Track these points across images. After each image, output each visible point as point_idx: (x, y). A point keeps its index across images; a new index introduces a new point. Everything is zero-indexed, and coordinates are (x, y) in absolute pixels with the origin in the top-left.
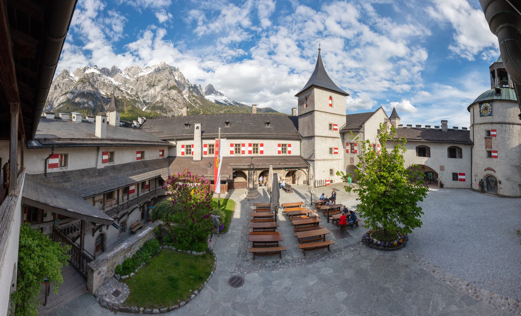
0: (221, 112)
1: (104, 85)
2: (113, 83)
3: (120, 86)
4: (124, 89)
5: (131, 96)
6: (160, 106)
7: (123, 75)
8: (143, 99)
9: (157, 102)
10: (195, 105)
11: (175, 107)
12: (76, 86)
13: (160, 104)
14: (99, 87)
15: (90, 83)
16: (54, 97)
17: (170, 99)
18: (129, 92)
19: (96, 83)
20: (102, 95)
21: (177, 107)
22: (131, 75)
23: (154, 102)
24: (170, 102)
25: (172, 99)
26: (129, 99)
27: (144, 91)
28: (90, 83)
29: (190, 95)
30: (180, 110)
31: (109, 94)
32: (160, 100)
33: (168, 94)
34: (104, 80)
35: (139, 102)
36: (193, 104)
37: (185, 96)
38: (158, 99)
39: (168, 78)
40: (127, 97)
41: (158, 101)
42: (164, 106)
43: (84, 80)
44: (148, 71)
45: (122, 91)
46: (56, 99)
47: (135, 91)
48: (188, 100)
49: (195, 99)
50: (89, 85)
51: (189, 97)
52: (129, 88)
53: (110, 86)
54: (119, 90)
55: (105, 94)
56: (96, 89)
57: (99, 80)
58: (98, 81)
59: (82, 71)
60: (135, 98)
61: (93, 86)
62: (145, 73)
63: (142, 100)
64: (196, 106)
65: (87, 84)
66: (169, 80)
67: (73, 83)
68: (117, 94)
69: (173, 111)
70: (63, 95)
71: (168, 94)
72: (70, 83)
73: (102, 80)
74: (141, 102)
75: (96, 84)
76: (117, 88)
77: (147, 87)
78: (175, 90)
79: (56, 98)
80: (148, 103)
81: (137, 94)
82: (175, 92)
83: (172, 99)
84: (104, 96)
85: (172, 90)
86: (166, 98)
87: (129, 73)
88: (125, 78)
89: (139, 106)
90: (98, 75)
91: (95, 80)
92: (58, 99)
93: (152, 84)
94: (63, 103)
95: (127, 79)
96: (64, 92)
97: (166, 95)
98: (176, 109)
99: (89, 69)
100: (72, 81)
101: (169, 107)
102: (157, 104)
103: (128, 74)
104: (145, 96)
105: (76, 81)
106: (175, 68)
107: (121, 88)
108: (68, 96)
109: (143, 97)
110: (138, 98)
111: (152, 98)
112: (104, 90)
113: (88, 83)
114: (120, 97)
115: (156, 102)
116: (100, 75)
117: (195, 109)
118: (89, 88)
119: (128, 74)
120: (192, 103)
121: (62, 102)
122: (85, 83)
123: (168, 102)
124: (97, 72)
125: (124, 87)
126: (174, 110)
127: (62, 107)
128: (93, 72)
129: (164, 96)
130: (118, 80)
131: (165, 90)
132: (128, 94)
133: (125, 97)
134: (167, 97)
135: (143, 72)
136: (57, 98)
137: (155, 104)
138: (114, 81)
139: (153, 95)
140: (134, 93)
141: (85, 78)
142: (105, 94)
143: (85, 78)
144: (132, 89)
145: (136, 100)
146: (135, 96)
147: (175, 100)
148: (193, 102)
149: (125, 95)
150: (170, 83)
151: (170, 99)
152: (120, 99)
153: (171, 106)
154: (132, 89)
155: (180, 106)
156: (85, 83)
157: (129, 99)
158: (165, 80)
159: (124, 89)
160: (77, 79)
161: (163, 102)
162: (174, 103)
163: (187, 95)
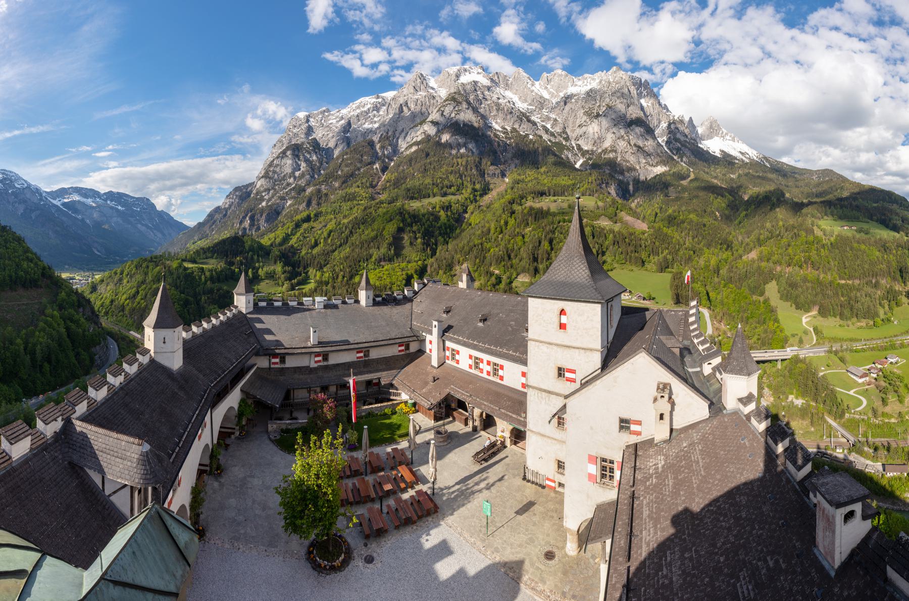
0: (732, 176)
1: (498, 110)
2: (517, 105)
3: (531, 112)
4: (539, 120)
5: (552, 134)
6: (610, 158)
7: (536, 91)
8: (578, 142)
9: (605, 151)
12: (442, 109)
13: (611, 155)
14: (488, 113)
15: (469, 103)
17: (630, 145)
18: (549, 126)
19: (481, 104)
20: (495, 130)
21: (644, 161)
22: (551, 90)
23: (600, 151)
24: (631, 151)
26: (550, 141)
27: (579, 126)
28: (469, 103)
29: (670, 138)
30: (650, 168)
31: (509, 129)
34: (499, 98)
35: (568, 149)
37: (660, 140)
38: (607, 144)
39: (625, 101)
40: (545, 137)
41: (606, 149)
42: (619, 159)
43: (457, 96)
44: (586, 85)
45: (534, 124)
46: (403, 135)
47: (562, 126)
48: (666, 149)
49: (680, 146)
50: (468, 109)
51: (668, 143)
52: (548, 118)
53: (511, 113)
54: (529, 121)
55: (500, 129)
56: (484, 117)
57: (488, 97)
58: (486, 100)
59: (454, 77)
60: (562, 139)
61: (475, 110)
62: (581, 88)
63: (574, 145)
64: (682, 161)
65: (465, 105)
66: (628, 106)
67: (435, 101)
68: (524, 129)
72: (430, 102)
73: (495, 98)
74: (573, 147)
75: (483, 106)
76: (524, 117)
77: (585, 118)
78: (640, 126)
79: (403, 131)
80: (587, 151)
81: (564, 132)
82: (640, 131)
84: (498, 133)
86: (623, 143)
87: (549, 86)
88: (541, 97)
89: (570, 156)
90: (485, 86)
91: (481, 96)
93: (595, 111)
94: (417, 143)
95: (545, 100)
98: (642, 165)
99: (467, 73)
100: (434, 98)
101: (628, 161)
102: (604, 155)
103: (546, 88)
105: (441, 98)
106: (641, 81)
107: (533, 118)
108: (426, 129)
109: (577, 139)
110: (567, 139)
111: (595, 142)
112: (499, 121)
113: (465, 103)
114: (531, 137)
115: (603, 151)
116: (489, 88)
117: (680, 168)
118: (467, 116)
119: (546, 88)
121: (414, 140)
122: (459, 103)
124: (484, 81)
125: (539, 116)
126: (638, 168)
127: (415, 152)
128: (476, 79)
129: (619, 138)
130: (525, 101)
132: (546, 130)
133: (541, 137)
134: (624, 140)
135: (576, 85)
137: (601, 153)
138: (519, 103)
139: (596, 135)
140: (558, 129)
141: (459, 93)
142: (500, 129)
143: (459, 93)
144: (555, 120)
145: (564, 143)
148: (677, 153)
149: (541, 132)
150: (631, 112)
151: (630, 145)
152: (531, 140)
154: (555, 120)
156: (459, 103)
157: (550, 141)
159: (539, 120)
160: (443, 93)
161: (616, 151)
163: (665, 138)
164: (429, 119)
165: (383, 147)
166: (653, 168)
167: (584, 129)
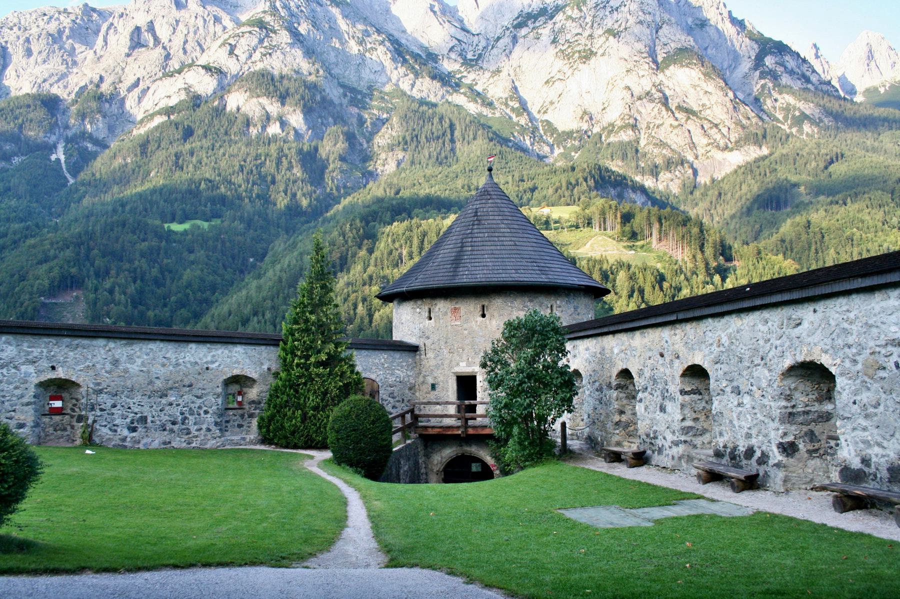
6: (621, 143)
9: (611, 129)
10: (794, 130)
11: (693, 146)
12: (233, 42)
13: (626, 136)
16: (130, 80)
21: (705, 141)
25: (679, 108)
36: (785, 127)
39: (649, 18)
42: (643, 143)
43: (268, 18)
46: (137, 92)
64: (801, 131)
65: (284, 37)
66: (658, 28)
69: (682, 162)
79: (136, 84)
85: (672, 68)
92: (145, 91)
94: (169, 111)
96: (175, 64)
97: (648, 93)
98: (701, 151)
101: (662, 144)
102: (608, 136)
104: (552, 103)
115: (604, 129)
120: (778, 120)
123: (658, 122)
126: (690, 158)
129: (640, 98)
131: (641, 73)
134: (652, 101)
136: (142, 86)
146: (506, 105)
147: (689, 112)
148: (786, 118)
150: (664, 40)
153: (676, 140)
155: (718, 137)
161: (634, 127)
162: (692, 125)
164: (202, 61)
166: (727, 154)
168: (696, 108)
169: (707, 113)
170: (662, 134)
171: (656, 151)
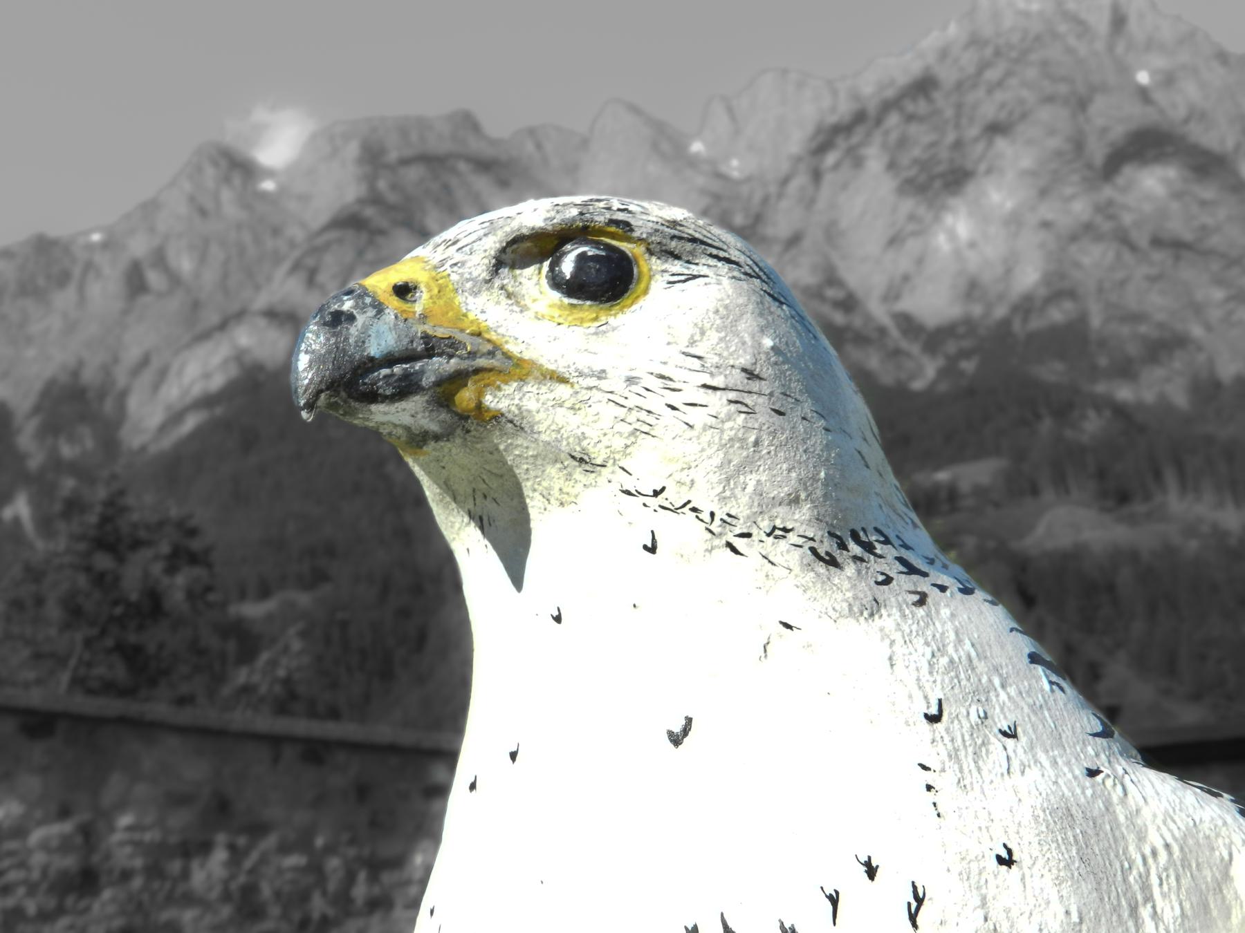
9: (1026, 306)
11: (1198, 309)
13: (1057, 315)
16: (132, 354)
17: (1133, 248)
21: (1218, 294)
24: (1144, 270)
25: (1157, 242)
32: (1047, 279)
33: (1106, 209)
42: (1096, 321)
43: (369, 212)
46: (147, 377)
66: (1082, 104)
70: (204, 336)
71: (1106, 209)
79: (145, 361)
81: (832, 279)
83: (1157, 242)
92: (163, 374)
94: (207, 401)
96: (213, 318)
98: (1215, 314)
101: (1136, 318)
102: (1025, 320)
123: (1120, 275)
126: (1197, 331)
127: (196, 434)
134: (1099, 237)
136: (156, 363)
147: (1178, 246)
151: (1133, 248)
153: (1158, 303)
158: (1045, 114)
161: (1071, 294)
164: (262, 301)
165: (52, 428)
167: (913, 246)
168: (1188, 236)
169: (1215, 241)
170: (1131, 300)
171: (1125, 330)
